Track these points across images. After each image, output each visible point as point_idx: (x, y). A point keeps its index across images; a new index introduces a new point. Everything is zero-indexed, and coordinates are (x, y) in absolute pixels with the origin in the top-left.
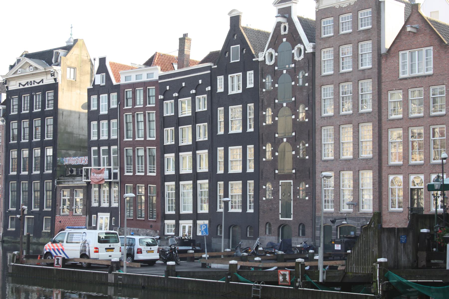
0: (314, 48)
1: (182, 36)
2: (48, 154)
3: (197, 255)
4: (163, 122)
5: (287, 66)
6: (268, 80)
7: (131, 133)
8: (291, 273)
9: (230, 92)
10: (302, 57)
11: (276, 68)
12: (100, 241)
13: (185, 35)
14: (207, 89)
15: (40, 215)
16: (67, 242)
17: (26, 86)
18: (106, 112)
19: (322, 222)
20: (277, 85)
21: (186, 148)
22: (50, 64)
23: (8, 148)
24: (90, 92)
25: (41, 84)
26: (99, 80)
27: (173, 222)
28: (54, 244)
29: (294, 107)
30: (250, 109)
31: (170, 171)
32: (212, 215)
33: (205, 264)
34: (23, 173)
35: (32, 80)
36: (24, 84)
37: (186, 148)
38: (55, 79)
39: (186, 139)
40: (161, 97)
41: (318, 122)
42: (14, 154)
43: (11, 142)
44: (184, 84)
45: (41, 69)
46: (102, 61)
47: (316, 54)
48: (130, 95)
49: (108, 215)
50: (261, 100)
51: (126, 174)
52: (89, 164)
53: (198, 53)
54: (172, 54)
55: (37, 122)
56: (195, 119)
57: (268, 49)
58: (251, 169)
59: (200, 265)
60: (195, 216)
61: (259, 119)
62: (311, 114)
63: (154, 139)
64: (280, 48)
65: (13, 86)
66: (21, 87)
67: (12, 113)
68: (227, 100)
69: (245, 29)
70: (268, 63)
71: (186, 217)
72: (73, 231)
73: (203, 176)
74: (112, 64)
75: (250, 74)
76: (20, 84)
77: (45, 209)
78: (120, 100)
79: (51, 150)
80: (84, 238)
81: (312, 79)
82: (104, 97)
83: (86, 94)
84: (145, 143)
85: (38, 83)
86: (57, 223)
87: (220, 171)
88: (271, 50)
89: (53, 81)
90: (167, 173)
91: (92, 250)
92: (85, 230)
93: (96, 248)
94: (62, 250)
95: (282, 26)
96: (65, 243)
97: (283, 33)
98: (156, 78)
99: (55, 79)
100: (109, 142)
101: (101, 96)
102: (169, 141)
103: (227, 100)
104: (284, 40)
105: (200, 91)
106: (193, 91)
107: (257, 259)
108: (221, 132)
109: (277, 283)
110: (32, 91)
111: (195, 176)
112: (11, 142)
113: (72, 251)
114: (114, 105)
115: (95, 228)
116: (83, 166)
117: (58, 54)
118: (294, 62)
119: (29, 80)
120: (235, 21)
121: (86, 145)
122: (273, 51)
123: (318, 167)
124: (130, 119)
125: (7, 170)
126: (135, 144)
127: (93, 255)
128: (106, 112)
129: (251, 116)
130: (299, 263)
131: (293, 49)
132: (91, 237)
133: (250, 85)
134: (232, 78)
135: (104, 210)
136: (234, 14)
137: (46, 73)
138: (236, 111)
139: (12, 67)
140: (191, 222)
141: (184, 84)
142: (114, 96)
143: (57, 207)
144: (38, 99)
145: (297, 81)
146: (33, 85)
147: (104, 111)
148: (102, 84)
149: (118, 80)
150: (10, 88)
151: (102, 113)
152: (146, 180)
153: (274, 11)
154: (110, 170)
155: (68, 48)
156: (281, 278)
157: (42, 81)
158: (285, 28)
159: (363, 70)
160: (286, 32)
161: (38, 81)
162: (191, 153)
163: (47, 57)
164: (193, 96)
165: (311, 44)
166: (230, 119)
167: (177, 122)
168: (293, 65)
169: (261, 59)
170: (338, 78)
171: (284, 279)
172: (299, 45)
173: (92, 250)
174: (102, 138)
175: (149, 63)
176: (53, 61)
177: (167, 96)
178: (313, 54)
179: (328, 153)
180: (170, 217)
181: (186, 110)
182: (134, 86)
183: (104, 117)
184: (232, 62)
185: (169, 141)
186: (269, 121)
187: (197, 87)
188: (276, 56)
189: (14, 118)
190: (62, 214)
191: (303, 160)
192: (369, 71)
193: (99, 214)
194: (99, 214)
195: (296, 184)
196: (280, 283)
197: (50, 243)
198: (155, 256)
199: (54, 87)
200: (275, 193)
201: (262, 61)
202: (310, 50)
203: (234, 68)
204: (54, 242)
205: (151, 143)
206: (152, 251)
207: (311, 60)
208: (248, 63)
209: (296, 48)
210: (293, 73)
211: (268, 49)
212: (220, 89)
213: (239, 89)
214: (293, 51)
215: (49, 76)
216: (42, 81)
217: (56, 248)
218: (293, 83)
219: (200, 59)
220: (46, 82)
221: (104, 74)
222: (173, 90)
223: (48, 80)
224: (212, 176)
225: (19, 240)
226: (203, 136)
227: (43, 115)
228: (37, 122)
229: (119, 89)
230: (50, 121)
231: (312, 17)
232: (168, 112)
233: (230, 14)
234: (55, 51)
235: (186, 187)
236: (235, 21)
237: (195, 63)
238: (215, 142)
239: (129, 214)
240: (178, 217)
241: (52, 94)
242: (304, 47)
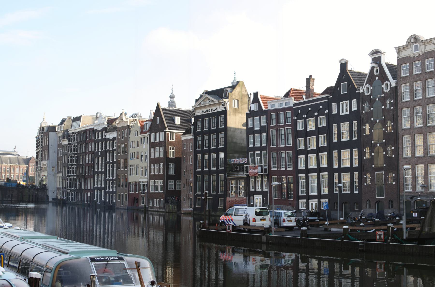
0: (397, 83)
1: (308, 77)
2: (221, 157)
3: (321, 223)
4: (297, 135)
5: (379, 96)
6: (366, 105)
7: (275, 142)
8: (384, 234)
9: (341, 114)
10: (389, 89)
11: (372, 97)
12: (257, 214)
13: (310, 76)
14: (325, 112)
15: (216, 197)
16: (235, 215)
17: (207, 113)
18: (259, 129)
20: (372, 109)
21: (312, 152)
22: (222, 98)
23: (196, 153)
24: (248, 116)
25: (216, 111)
26: (253, 107)
27: (305, 201)
28: (226, 216)
29: (384, 123)
30: (355, 125)
31: (302, 167)
32: (331, 196)
33: (327, 229)
34: (205, 169)
35: (210, 109)
36: (205, 111)
37: (312, 152)
38: (225, 108)
39: (313, 146)
40: (295, 118)
41: (400, 132)
42: (199, 157)
43: (197, 149)
44: (310, 109)
45: (216, 101)
46: (256, 95)
47: (398, 87)
48: (274, 117)
49: (261, 197)
50: (362, 119)
51: (273, 169)
52: (248, 163)
53: (319, 88)
54: (302, 89)
55: (214, 136)
56: (318, 132)
57: (366, 85)
58: (356, 165)
59: (323, 229)
60: (319, 197)
61: (360, 131)
62: (396, 127)
63: (291, 146)
64: (374, 83)
65: (198, 113)
66: (203, 113)
67: (197, 131)
68: (339, 119)
69: (350, 71)
70: (366, 94)
71: (313, 197)
72: (238, 207)
73: (324, 170)
74: (262, 97)
75: (354, 102)
77: (220, 193)
78: (268, 121)
79: (223, 154)
80: (246, 212)
81: (395, 104)
82: (257, 118)
83: (245, 117)
84: (286, 149)
85: (214, 110)
86: (228, 202)
87: (336, 166)
88: (368, 85)
89: (223, 109)
90: (300, 168)
91: (251, 220)
92: (247, 207)
93: (254, 219)
94: (232, 220)
95: (375, 69)
96: (233, 216)
97: (375, 74)
98: (291, 105)
99: (225, 108)
100: (261, 148)
101: (255, 118)
102: (301, 147)
103: (339, 119)
104: (377, 78)
106: (317, 114)
107: (361, 224)
108: (335, 140)
109: (375, 240)
110: (210, 116)
111: (319, 170)
112: (197, 149)
113: (238, 220)
114: (264, 124)
115: (252, 206)
116: (244, 164)
117: (226, 91)
118: (384, 93)
119: (208, 109)
120: (344, 66)
121: (246, 150)
122: (369, 86)
123: (401, 163)
124: (274, 133)
125: (195, 168)
126: (279, 150)
127: (252, 224)
128: (259, 129)
129: (355, 129)
130: (390, 226)
131: (383, 84)
132: (251, 211)
133: (354, 109)
134: (342, 104)
136: (343, 62)
137: (219, 104)
138: (345, 126)
139: (197, 101)
140: (317, 200)
141: (310, 109)
142: (264, 117)
143: (228, 192)
144: (214, 121)
145: (386, 106)
146: (211, 112)
147: (257, 128)
148: (256, 110)
149: (266, 107)
150: (196, 114)
151: (255, 129)
152: (286, 173)
153: (370, 59)
154: (261, 167)
155: (233, 87)
156: (378, 237)
157: (217, 109)
158: (377, 70)
159: (429, 98)
160: (378, 73)
161: (214, 109)
162: (315, 154)
163: (220, 94)
164: (317, 117)
165: (395, 81)
166: (341, 132)
167: (306, 134)
168: (383, 95)
169: (361, 91)
170: (413, 104)
171: (380, 237)
172: (387, 82)
173: (251, 220)
174: (256, 146)
175: (287, 95)
176: (224, 96)
177: (299, 117)
178: (396, 87)
179: (408, 154)
180: (303, 197)
181: (312, 126)
182: (277, 111)
183: (257, 132)
184: (342, 93)
185: (301, 147)
186: (367, 132)
187: (319, 111)
188: (371, 89)
189: (199, 133)
190: (230, 196)
191: (391, 157)
192: (433, 99)
193: (255, 196)
194: (255, 196)
195: (386, 174)
196: (377, 240)
197: (223, 216)
198: (294, 224)
199: (224, 113)
200: (373, 180)
201: (362, 93)
202: (394, 85)
203: (344, 98)
204: (226, 215)
205: (289, 149)
206: (291, 221)
207: (395, 92)
208: (352, 94)
209: (384, 84)
210: (383, 101)
211: (366, 85)
212: (335, 112)
213: (347, 112)
214: (383, 86)
215: (221, 106)
216: (217, 109)
217: (228, 218)
218: (383, 107)
219: (321, 92)
220: (219, 110)
221: (257, 103)
222: (302, 113)
223: (221, 108)
224: (330, 169)
225: (203, 213)
226: (323, 144)
227: (217, 131)
228: (214, 136)
229: (267, 113)
230: (222, 135)
231: (395, 63)
232: (300, 128)
233: (339, 62)
234: (224, 89)
235: (313, 177)
236: (344, 66)
237: (317, 94)
238: (331, 147)
239: (275, 195)
240: (308, 197)
241: (223, 117)
242: (390, 83)
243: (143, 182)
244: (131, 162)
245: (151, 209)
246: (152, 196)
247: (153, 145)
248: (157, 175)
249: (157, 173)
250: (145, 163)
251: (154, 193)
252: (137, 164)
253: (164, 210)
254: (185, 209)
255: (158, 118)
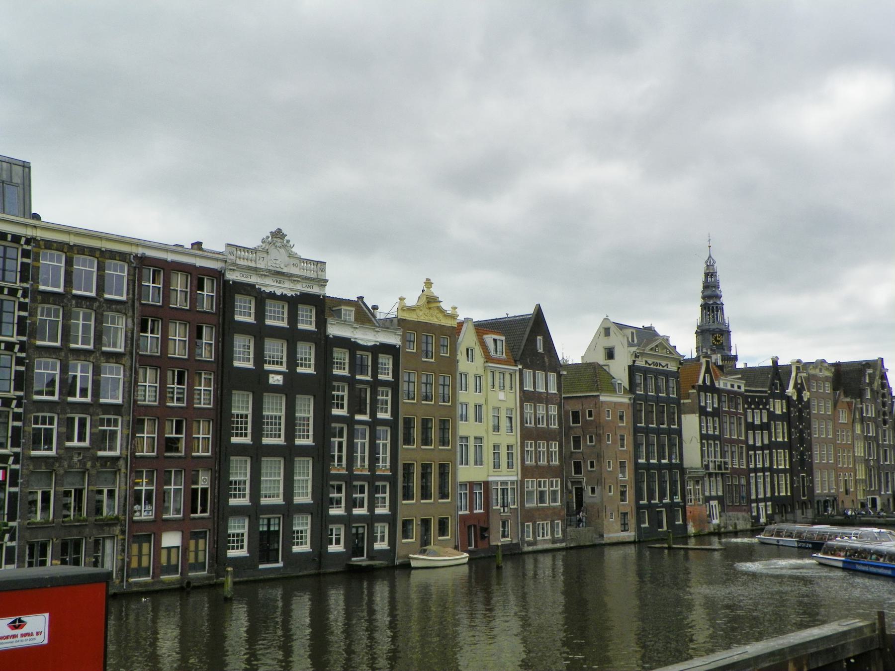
17: (652, 366)
19: (816, 499)
25: (665, 368)
35: (658, 361)
76: (646, 362)
105: (764, 408)
110: (657, 373)
135: (713, 498)
164: (761, 410)
185: (751, 442)
226: (766, 442)
232: (750, 420)
243: (504, 483)
244: (467, 428)
245: (530, 548)
246: (529, 516)
247: (527, 397)
248: (543, 467)
249: (543, 462)
250: (509, 438)
251: (538, 509)
252: (478, 435)
253: (564, 545)
254: (612, 535)
255: (540, 338)
